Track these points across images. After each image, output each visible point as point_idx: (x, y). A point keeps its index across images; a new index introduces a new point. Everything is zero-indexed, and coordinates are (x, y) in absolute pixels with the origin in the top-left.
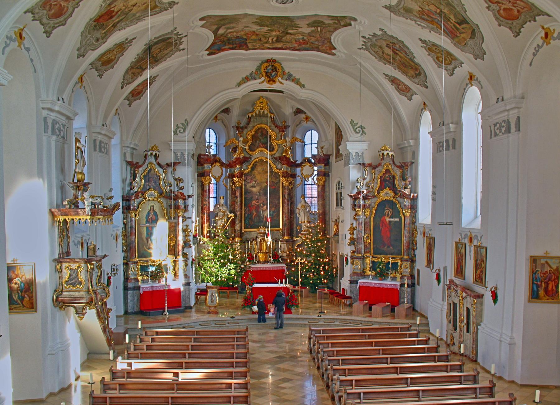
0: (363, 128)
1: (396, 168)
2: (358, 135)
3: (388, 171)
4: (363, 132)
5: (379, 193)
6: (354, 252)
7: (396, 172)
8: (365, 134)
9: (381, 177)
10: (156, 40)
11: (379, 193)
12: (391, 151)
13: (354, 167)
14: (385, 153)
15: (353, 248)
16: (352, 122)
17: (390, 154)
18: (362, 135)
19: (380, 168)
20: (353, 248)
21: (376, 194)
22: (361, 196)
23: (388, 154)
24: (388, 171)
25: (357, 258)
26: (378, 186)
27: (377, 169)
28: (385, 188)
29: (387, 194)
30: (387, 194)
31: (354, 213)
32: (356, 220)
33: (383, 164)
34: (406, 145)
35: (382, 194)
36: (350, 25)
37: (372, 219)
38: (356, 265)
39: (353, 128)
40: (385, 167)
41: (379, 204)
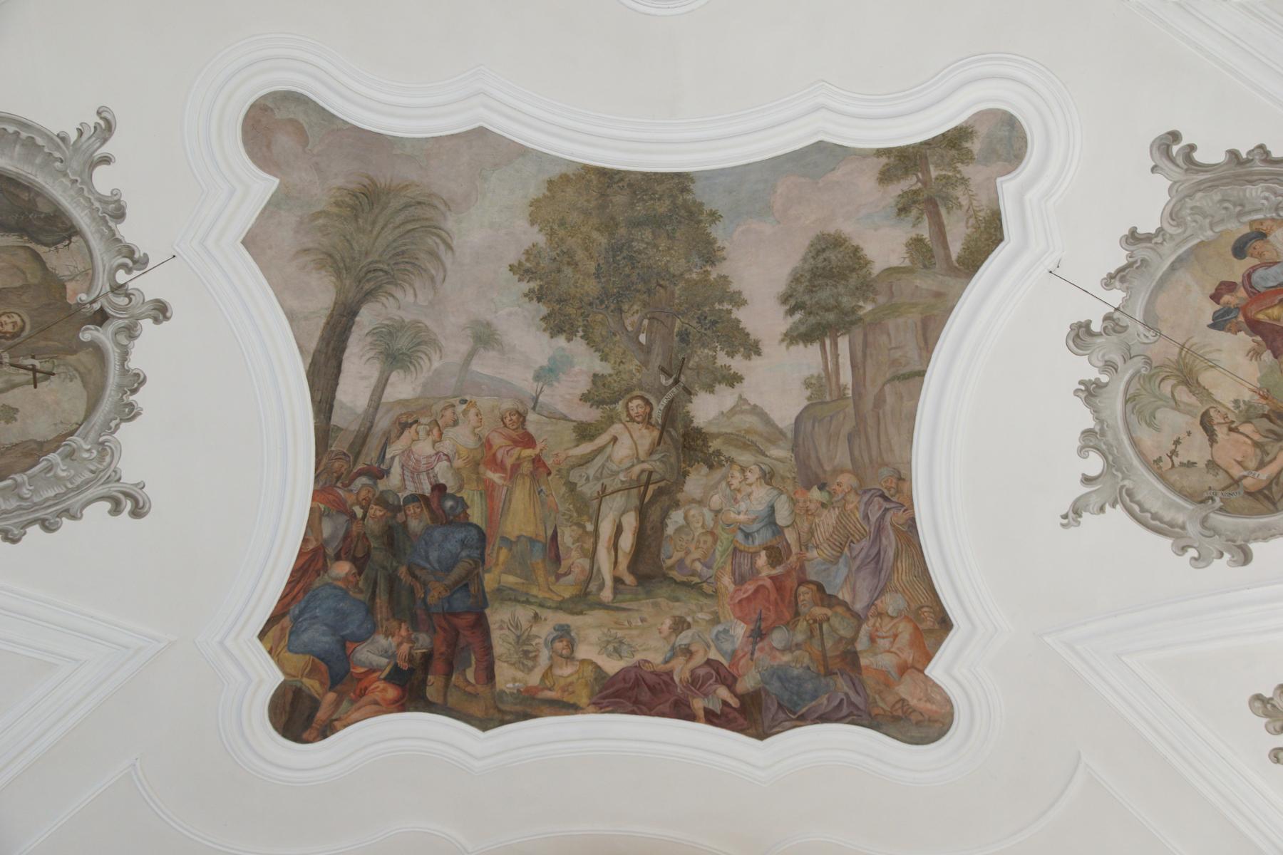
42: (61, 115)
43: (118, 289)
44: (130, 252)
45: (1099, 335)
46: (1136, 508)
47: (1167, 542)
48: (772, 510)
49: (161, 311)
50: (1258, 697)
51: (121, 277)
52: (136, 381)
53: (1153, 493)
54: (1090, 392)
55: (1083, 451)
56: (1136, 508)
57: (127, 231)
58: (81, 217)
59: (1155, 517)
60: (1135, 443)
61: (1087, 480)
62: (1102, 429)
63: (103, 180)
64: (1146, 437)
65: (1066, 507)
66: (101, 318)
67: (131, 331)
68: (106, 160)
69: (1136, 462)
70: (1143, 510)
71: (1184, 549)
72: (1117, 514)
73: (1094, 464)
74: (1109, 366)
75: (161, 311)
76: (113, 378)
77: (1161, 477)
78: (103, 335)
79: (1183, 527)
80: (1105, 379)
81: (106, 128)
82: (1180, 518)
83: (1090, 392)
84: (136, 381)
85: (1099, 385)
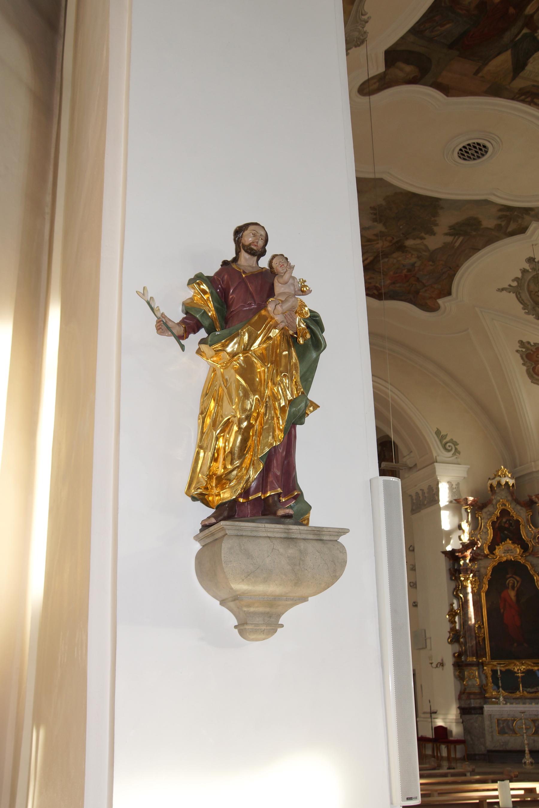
0: (455, 444)
1: (519, 507)
2: (450, 454)
3: (504, 512)
4: (456, 449)
5: (492, 549)
6: (460, 655)
7: (520, 514)
8: (459, 453)
9: (493, 523)
11: (492, 549)
12: (512, 478)
13: (446, 508)
14: (503, 483)
15: (457, 648)
16: (438, 433)
17: (511, 482)
18: (454, 454)
19: (490, 508)
20: (457, 648)
21: (486, 551)
22: (468, 553)
23: (507, 483)
24: (504, 512)
25: (471, 665)
26: (490, 535)
27: (485, 510)
28: (505, 540)
29: (508, 551)
30: (508, 551)
31: (453, 585)
32: (457, 597)
33: (494, 502)
34: (534, 470)
35: (499, 551)
36: (523, 230)
37: (483, 595)
38: (470, 679)
39: (441, 442)
40: (499, 507)
41: (494, 569)
45: (536, 262)
46: (519, 296)
47: (522, 306)
48: (415, 263)
50: (522, 341)
53: (525, 296)
54: (524, 271)
55: (513, 281)
56: (519, 296)
59: (522, 300)
60: (528, 285)
61: (510, 286)
62: (522, 279)
64: (532, 286)
65: (501, 287)
69: (526, 288)
70: (520, 297)
71: (525, 309)
72: (513, 295)
73: (515, 284)
74: (534, 269)
77: (530, 295)
79: (528, 305)
80: (530, 270)
82: (528, 304)
83: (524, 271)
85: (528, 271)
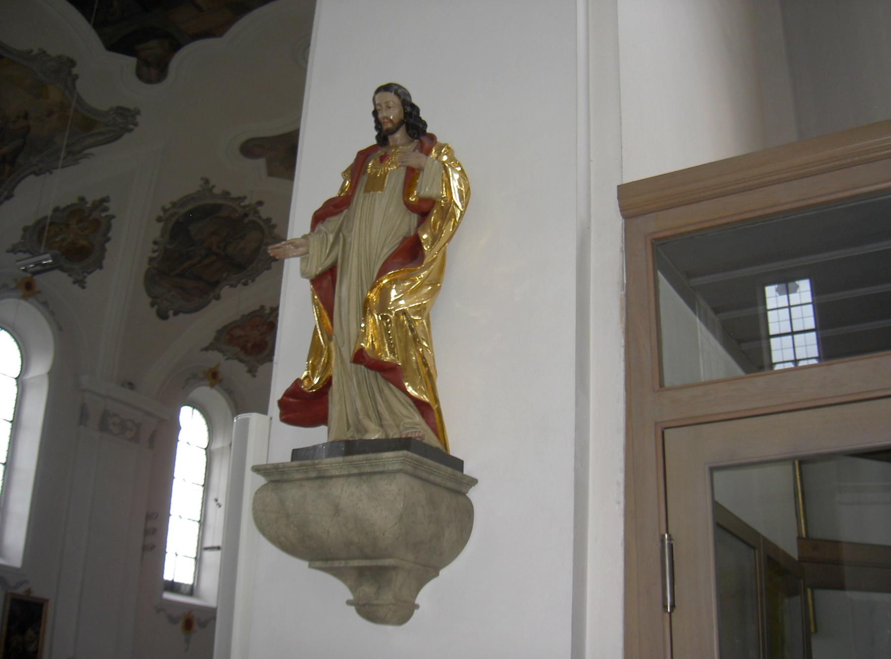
10: (183, 211)
42: (192, 186)
43: (244, 207)
44: (239, 198)
49: (260, 203)
51: (242, 204)
52: (268, 220)
57: (234, 194)
58: (221, 202)
63: (217, 191)
66: (246, 215)
67: (256, 212)
68: (214, 187)
75: (260, 203)
76: (262, 224)
78: (251, 217)
81: (207, 181)
84: (268, 220)
